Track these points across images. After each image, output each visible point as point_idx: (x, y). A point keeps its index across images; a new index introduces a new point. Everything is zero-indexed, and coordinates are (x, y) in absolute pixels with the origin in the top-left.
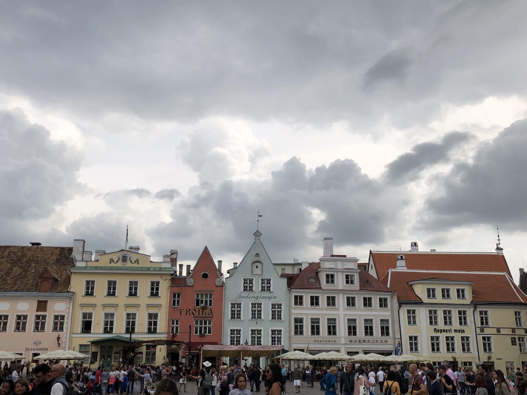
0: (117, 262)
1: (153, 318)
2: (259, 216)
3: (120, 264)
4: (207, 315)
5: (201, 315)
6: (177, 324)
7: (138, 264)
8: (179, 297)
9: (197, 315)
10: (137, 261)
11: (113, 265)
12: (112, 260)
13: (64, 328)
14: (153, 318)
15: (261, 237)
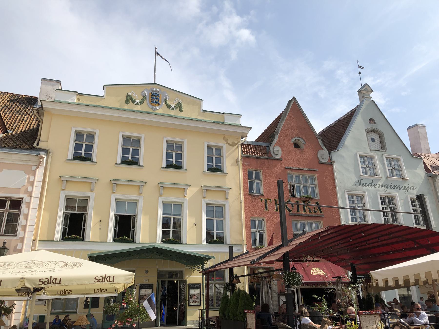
0: (141, 103)
1: (215, 212)
2: (360, 67)
3: (146, 107)
4: (313, 213)
5: (302, 212)
6: (261, 227)
7: (181, 111)
8: (258, 178)
9: (295, 211)
10: (179, 106)
11: (131, 106)
12: (129, 99)
13: (19, 229)
14: (215, 212)
15: (371, 95)
